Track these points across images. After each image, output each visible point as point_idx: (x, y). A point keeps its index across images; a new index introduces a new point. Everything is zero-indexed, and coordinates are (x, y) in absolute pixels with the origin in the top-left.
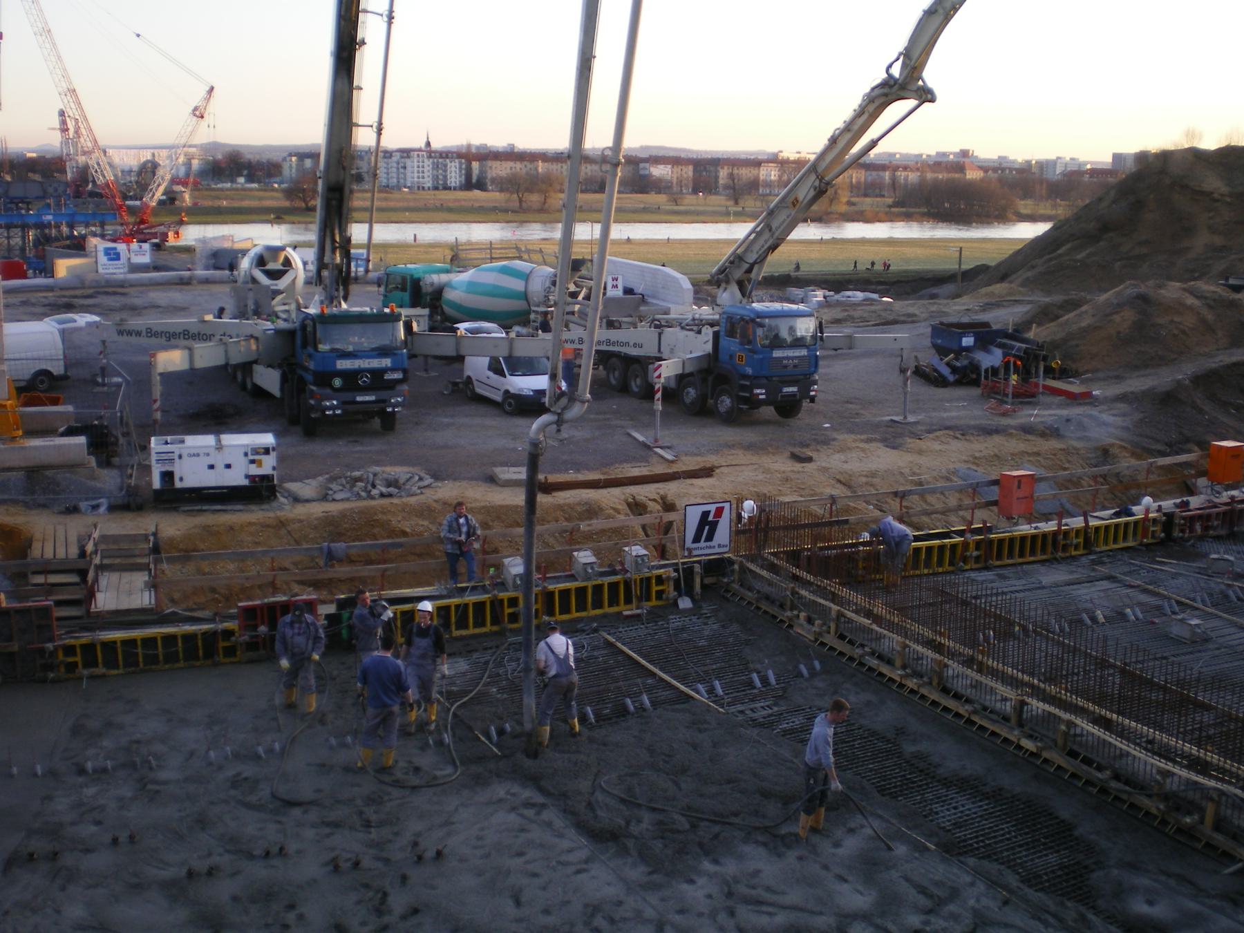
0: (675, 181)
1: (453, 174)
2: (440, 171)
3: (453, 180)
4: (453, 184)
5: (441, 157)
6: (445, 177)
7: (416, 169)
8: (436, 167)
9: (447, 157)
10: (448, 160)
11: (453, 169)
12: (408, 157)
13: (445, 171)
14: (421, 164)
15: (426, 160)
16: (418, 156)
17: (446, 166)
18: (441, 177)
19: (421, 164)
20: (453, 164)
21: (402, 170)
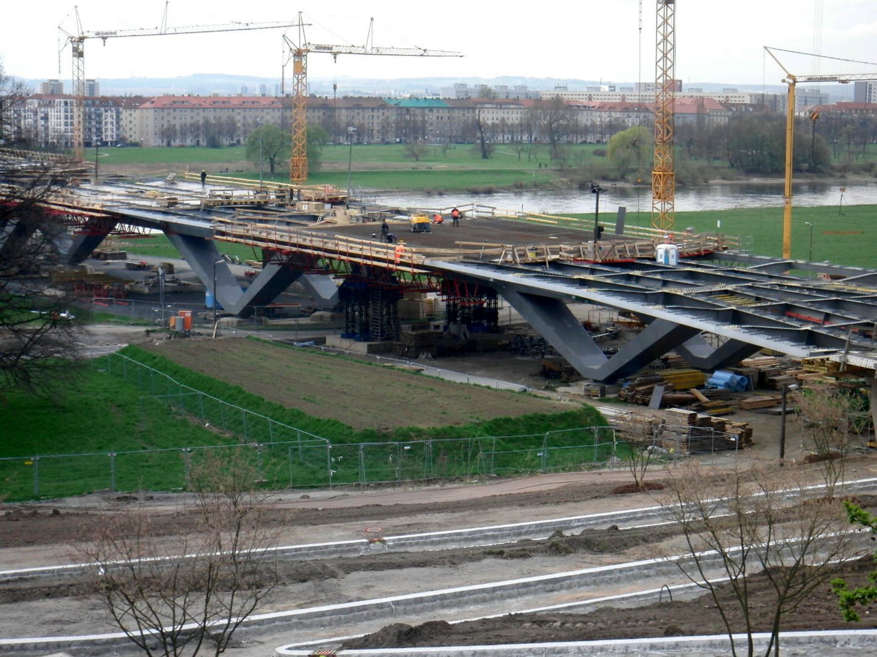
0: (376, 128)
1: (109, 126)
2: (93, 123)
3: (109, 133)
4: (109, 139)
5: (94, 104)
6: (99, 130)
7: (63, 121)
8: (88, 117)
9: (101, 105)
10: (102, 109)
11: (109, 120)
12: (50, 104)
13: (100, 123)
14: (69, 114)
15: (75, 109)
16: (66, 103)
17: (100, 116)
18: (94, 130)
19: (69, 114)
20: (109, 113)
21: (43, 122)
